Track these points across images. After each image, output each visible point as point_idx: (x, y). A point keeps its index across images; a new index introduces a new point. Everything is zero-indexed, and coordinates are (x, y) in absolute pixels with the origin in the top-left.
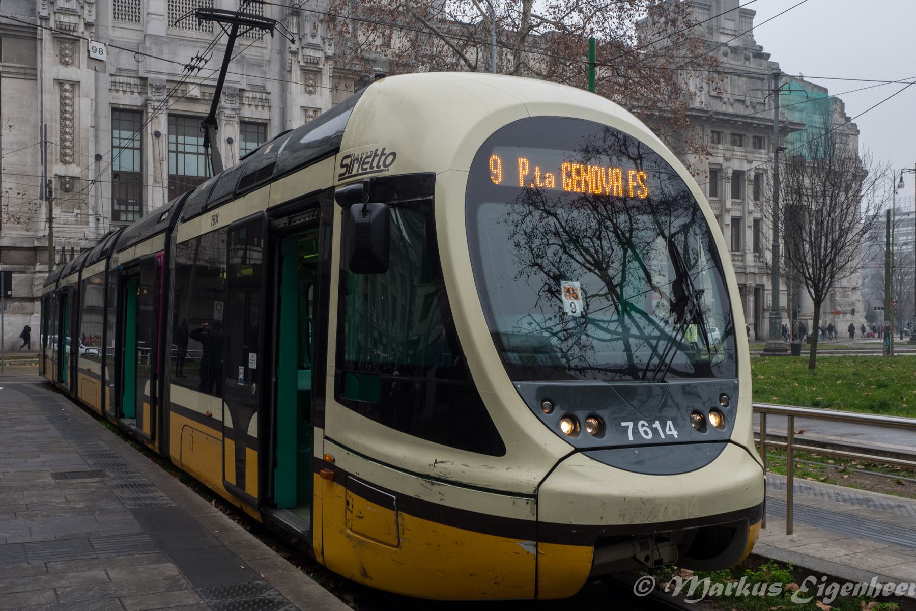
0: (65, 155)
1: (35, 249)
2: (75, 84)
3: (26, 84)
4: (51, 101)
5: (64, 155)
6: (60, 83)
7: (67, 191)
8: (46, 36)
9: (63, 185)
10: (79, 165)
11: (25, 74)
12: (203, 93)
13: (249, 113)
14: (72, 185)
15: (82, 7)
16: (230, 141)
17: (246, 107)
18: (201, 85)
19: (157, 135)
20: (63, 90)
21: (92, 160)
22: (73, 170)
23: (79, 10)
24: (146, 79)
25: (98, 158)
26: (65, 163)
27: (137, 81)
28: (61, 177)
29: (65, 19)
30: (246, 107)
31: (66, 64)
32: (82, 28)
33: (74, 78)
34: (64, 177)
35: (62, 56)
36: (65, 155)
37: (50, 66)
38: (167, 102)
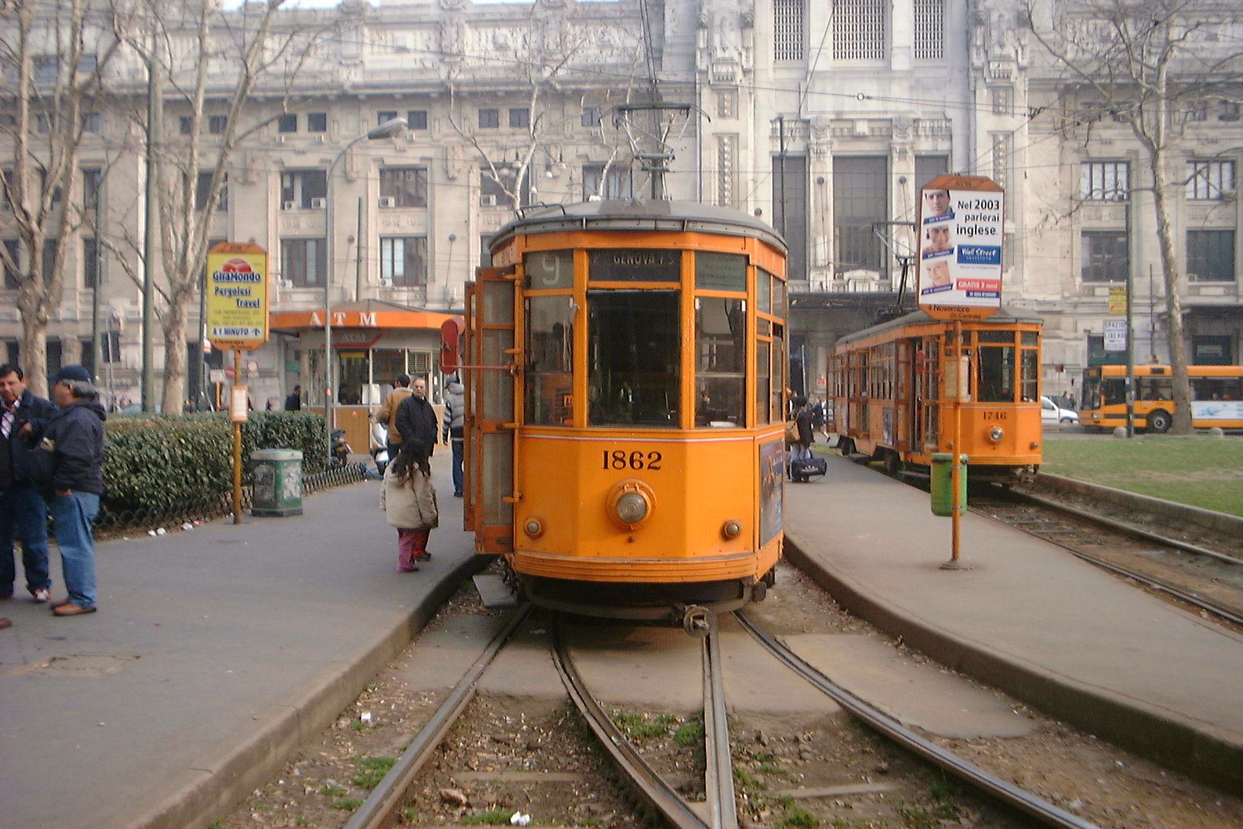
2: (734, 137)
4: (711, 159)
6: (719, 137)
12: (872, 130)
13: (925, 146)
16: (903, 181)
17: (923, 139)
18: (870, 120)
19: (821, 181)
20: (722, 145)
23: (736, 58)
24: (807, 122)
27: (799, 125)
29: (723, 70)
30: (923, 139)
32: (740, 75)
33: (734, 130)
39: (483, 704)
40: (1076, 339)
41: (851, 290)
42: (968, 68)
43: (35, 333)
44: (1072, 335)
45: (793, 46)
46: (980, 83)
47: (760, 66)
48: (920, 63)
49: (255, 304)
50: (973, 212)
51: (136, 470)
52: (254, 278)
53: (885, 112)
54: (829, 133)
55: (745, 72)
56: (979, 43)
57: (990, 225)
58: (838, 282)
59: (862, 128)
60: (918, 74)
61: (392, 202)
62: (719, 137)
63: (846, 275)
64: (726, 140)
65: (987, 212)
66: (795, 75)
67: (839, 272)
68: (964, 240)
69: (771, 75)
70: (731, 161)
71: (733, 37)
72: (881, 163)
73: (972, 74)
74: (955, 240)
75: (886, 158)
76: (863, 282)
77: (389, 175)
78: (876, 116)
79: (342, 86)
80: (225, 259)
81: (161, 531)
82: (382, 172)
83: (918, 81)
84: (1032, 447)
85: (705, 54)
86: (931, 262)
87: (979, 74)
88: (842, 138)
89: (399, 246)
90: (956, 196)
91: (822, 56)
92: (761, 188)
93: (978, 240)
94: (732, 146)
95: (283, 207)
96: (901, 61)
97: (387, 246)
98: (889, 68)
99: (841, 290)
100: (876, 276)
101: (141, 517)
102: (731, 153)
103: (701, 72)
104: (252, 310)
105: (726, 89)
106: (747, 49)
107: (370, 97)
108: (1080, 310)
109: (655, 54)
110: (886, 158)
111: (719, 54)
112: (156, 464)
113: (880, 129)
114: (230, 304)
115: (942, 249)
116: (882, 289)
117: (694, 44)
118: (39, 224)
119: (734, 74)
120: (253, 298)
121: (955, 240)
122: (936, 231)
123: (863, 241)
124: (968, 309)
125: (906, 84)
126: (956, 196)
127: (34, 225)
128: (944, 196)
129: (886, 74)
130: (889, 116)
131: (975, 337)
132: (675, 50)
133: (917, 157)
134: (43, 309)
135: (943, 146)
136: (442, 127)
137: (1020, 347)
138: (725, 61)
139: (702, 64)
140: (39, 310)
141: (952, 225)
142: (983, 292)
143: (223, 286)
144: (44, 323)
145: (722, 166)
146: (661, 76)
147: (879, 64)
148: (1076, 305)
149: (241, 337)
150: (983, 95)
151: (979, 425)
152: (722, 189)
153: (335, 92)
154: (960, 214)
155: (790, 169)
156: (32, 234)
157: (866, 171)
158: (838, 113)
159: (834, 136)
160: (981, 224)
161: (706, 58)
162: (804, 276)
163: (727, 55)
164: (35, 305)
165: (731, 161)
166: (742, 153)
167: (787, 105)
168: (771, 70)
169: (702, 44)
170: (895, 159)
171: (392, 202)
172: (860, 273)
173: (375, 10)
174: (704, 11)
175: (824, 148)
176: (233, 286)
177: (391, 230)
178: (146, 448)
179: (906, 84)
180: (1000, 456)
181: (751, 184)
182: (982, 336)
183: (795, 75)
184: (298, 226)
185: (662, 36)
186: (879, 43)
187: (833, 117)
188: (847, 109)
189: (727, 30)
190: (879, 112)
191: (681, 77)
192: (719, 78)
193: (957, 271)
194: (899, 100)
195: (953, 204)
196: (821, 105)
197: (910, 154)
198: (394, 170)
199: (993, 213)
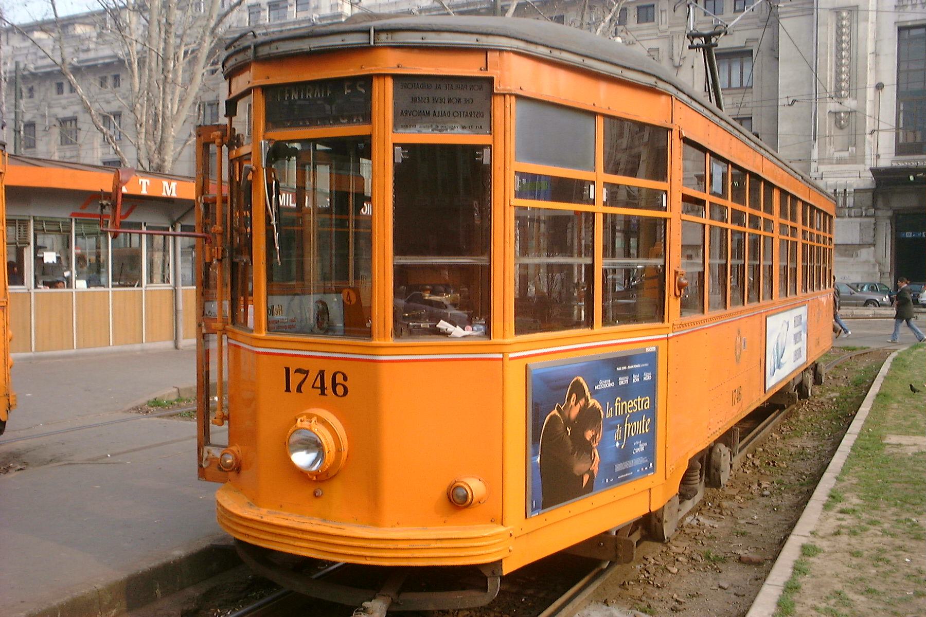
0: (841, 89)
3: (804, 20)
4: (827, 34)
7: (841, 128)
11: (803, 10)
14: (848, 121)
20: (840, 19)
21: (870, 93)
22: (850, 104)
25: (879, 87)
34: (839, 113)
36: (841, 89)
64: (844, 14)
70: (849, 35)
92: (882, 58)
94: (850, 20)
102: (850, 27)
145: (839, 42)
152: (839, 65)
165: (849, 35)
166: (861, 26)
181: (870, 58)
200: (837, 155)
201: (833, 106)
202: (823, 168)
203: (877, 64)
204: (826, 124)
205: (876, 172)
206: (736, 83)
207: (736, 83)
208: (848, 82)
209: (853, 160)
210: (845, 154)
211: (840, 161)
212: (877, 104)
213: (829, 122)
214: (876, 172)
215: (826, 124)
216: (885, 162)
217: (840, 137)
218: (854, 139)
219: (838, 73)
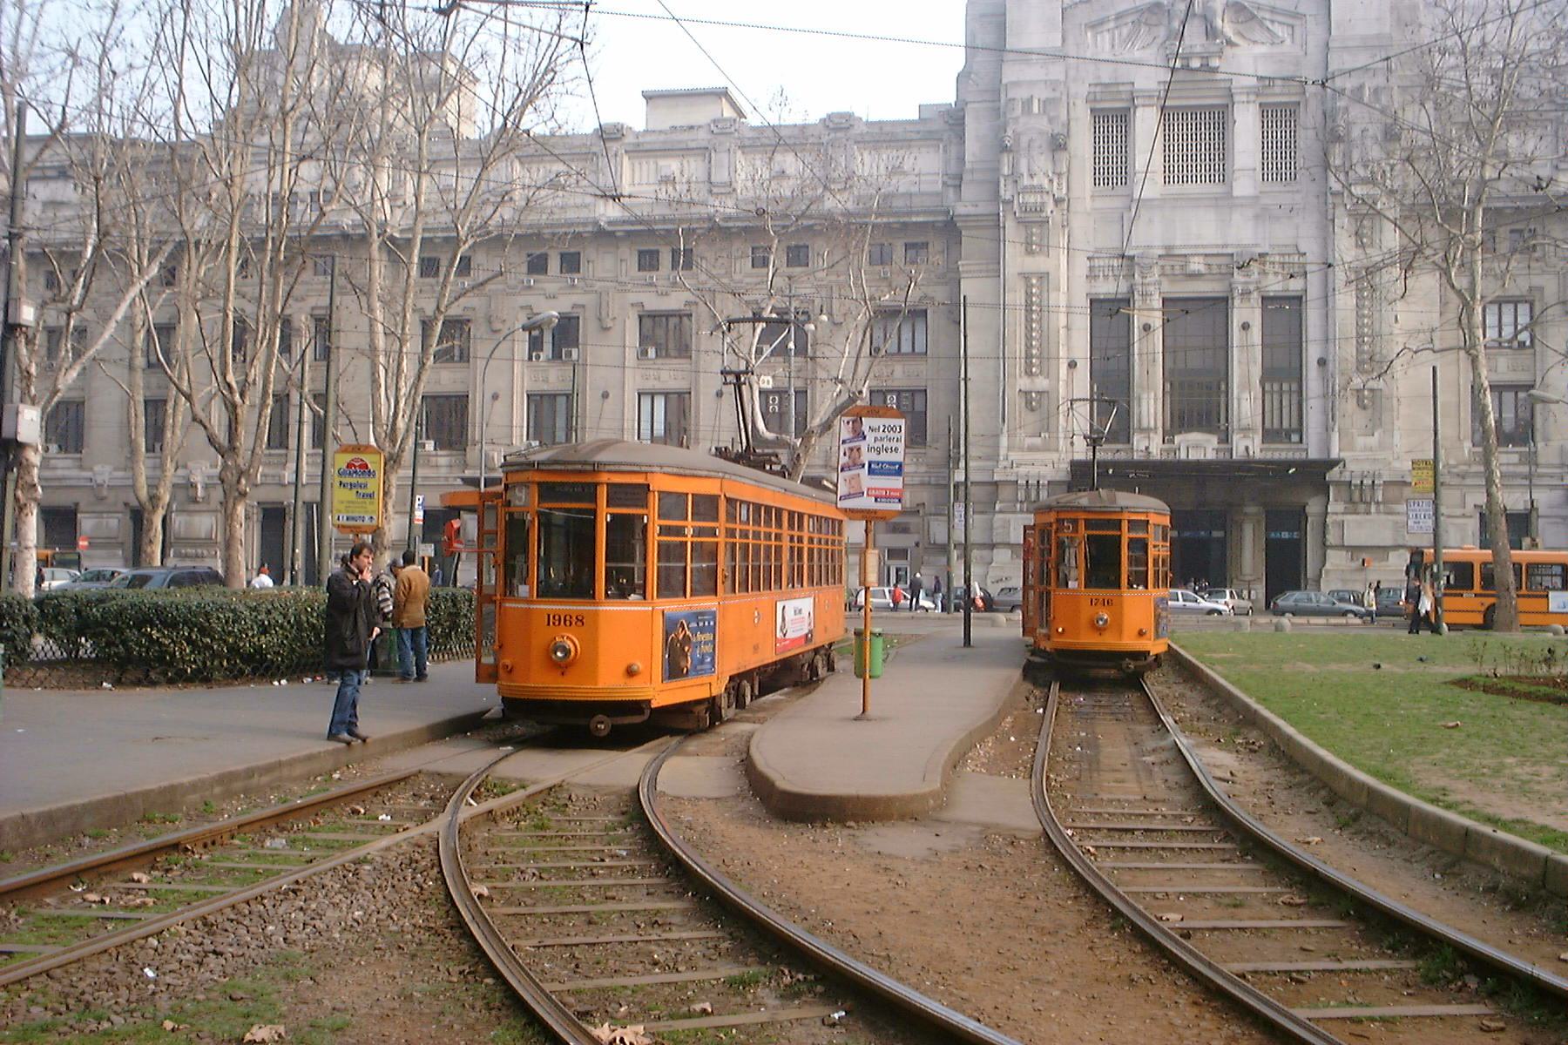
1: (996, 484)
2: (1043, 276)
5: (1029, 365)
6: (1026, 277)
7: (1032, 410)
8: (1010, 224)
9: (1028, 403)
10: (1048, 377)
13: (1274, 285)
14: (1039, 402)
15: (1051, 181)
16: (1245, 327)
17: (1271, 276)
19: (1147, 328)
20: (1029, 286)
22: (1041, 383)
24: (1132, 258)
25: (1072, 365)
26: (1029, 373)
28: (1027, 393)
29: (1031, 199)
30: (1271, 276)
31: (1030, 252)
32: (1050, 206)
33: (1043, 269)
35: (1029, 244)
37: (1015, 260)
38: (1160, 283)
39: (421, 777)
40: (1464, 516)
41: (1183, 456)
42: (1326, 192)
43: (234, 507)
44: (1459, 512)
45: (1114, 169)
46: (1340, 211)
47: (1075, 193)
48: (1268, 187)
49: (371, 496)
50: (880, 434)
51: (264, 631)
52: (371, 474)
53: (1225, 246)
54: (1156, 270)
55: (1057, 202)
56: (1338, 162)
57: (894, 444)
58: (1166, 446)
59: (1197, 265)
60: (1266, 201)
61: (652, 352)
62: (1026, 277)
63: (1177, 439)
65: (892, 435)
66: (1118, 203)
67: (1168, 435)
68: (874, 457)
69: (1088, 203)
71: (1042, 162)
72: (1222, 304)
73: (1330, 199)
74: (866, 457)
75: (1226, 300)
76: (1199, 447)
77: (648, 322)
78: (1215, 251)
79: (596, 223)
80: (348, 457)
81: (284, 682)
82: (640, 318)
83: (1265, 209)
84: (1141, 634)
85: (1010, 181)
86: (847, 474)
87: (1338, 200)
88: (1173, 277)
89: (660, 403)
90: (867, 422)
91: (1151, 183)
92: (1075, 334)
93: (884, 457)
95: (530, 358)
96: (1243, 186)
97: (646, 402)
98: (1229, 195)
99: (1171, 456)
100: (1214, 440)
101: (267, 669)
102: (1040, 296)
103: (1006, 202)
104: (368, 500)
105: (1034, 221)
106: (1059, 175)
107: (629, 233)
108: (1468, 481)
109: (956, 181)
110: (1226, 300)
111: (1026, 181)
112: (282, 627)
113: (1219, 266)
114: (350, 495)
115: (855, 464)
116: (1221, 456)
117: (997, 170)
118: (242, 395)
119: (1043, 204)
120: (368, 491)
121: (866, 457)
122: (851, 449)
123: (1198, 402)
124: (875, 512)
125: (1250, 213)
126: (867, 422)
127: (237, 397)
128: (858, 421)
129: (1226, 201)
130: (1229, 251)
131: (1082, 525)
132: (977, 176)
133: (1265, 300)
134: (243, 481)
135: (1295, 285)
136: (711, 263)
137: (1126, 536)
138: (1033, 190)
139: (1006, 192)
140: (239, 482)
141: (864, 445)
142: (888, 498)
143: (347, 480)
144: (243, 495)
146: (961, 209)
147: (1217, 189)
148: (1463, 476)
149: (359, 523)
150: (1343, 221)
151: (1086, 611)
152: (1029, 338)
153: (590, 229)
154: (870, 437)
155: (1110, 314)
156: (235, 406)
157: (1200, 316)
158: (1168, 248)
159: (1163, 275)
160: (887, 444)
161: (1009, 187)
162: (1128, 440)
163: (1035, 182)
164: (235, 479)
165: (1040, 305)
166: (1053, 295)
167: (1109, 239)
168: (1088, 199)
169: (1006, 171)
170: (1237, 302)
171: (652, 352)
172: (1195, 437)
173: (637, 135)
174: (1010, 133)
175: (1152, 288)
176: (354, 480)
177: (650, 385)
178: (275, 614)
179: (1250, 213)
180: (1108, 642)
181: (1062, 332)
182: (1089, 524)
183: (1118, 203)
184: (546, 381)
185: (961, 159)
186: (1218, 164)
187: (1161, 252)
188: (1178, 243)
189: (1035, 153)
190: (1217, 246)
191: (982, 209)
192: (1026, 209)
193: (867, 481)
194: (1242, 233)
195: (865, 428)
196: (1149, 236)
197: (1255, 295)
198: (655, 316)
199: (897, 435)
200: (1029, 441)
201: (1024, 383)
202: (1014, 456)
203: (1069, 337)
204: (1015, 403)
205: (1073, 464)
206: (906, 348)
207: (906, 348)
208: (1038, 359)
209: (1045, 448)
210: (1037, 441)
211: (1031, 449)
212: (1070, 382)
213: (1020, 402)
214: (1073, 464)
215: (1015, 403)
216: (1081, 451)
217: (1030, 418)
218: (1046, 425)
219: (1029, 347)
